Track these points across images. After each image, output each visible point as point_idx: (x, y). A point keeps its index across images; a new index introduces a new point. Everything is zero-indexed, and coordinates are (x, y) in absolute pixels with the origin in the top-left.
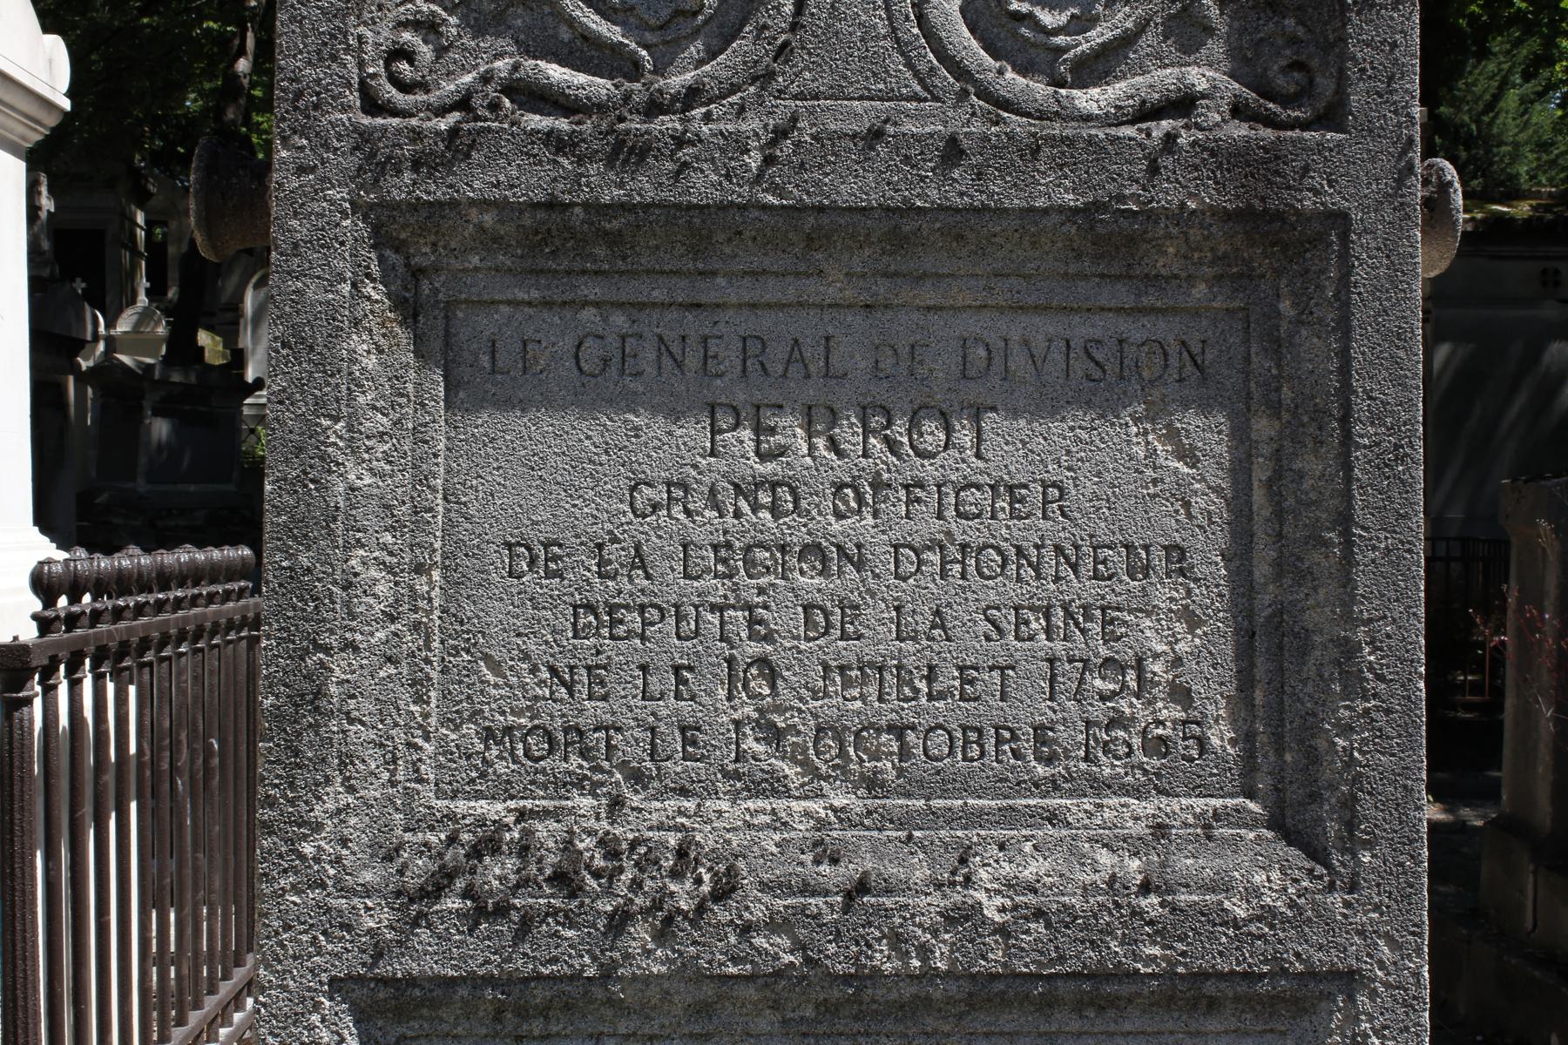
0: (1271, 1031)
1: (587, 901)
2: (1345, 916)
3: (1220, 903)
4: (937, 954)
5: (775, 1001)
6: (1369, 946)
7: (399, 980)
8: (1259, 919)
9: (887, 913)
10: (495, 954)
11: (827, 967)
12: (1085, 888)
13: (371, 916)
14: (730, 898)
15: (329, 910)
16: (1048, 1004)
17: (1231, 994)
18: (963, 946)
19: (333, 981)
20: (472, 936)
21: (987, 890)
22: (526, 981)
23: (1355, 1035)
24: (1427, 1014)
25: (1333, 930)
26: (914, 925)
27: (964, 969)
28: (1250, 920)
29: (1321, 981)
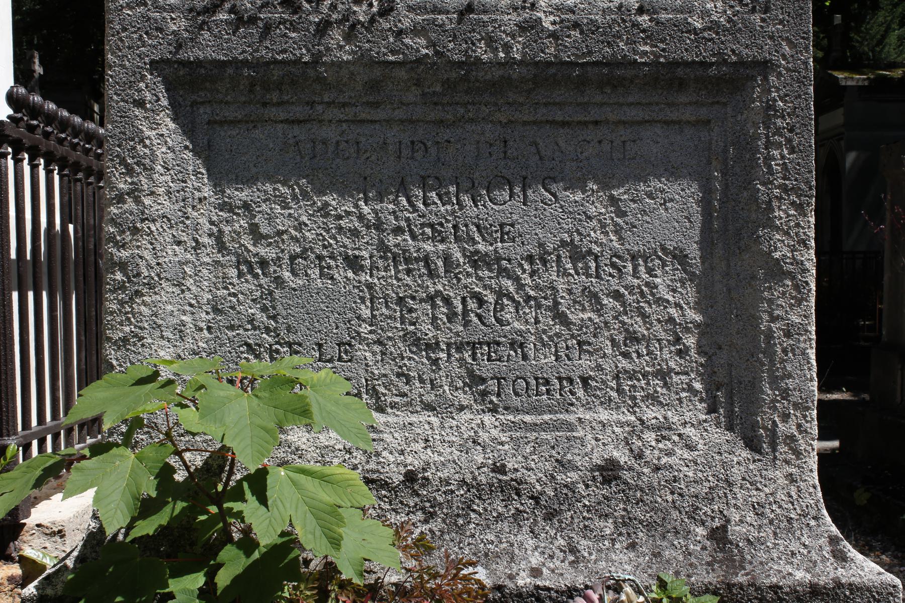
0: (718, 102)
1: (304, 15)
2: (762, 27)
3: (686, 19)
4: (515, 49)
5: (418, 80)
6: (776, 45)
7: (191, 62)
8: (710, 29)
9: (484, 24)
10: (248, 47)
11: (448, 56)
12: (604, 11)
13: (175, 23)
14: (390, 15)
15: (149, 19)
16: (581, 84)
17: (692, 77)
18: (530, 44)
19: (152, 62)
20: (234, 36)
21: (545, 12)
22: (268, 64)
23: (768, 101)
24: (812, 88)
25: (755, 35)
26: (501, 31)
27: (531, 59)
28: (704, 29)
29: (747, 68)
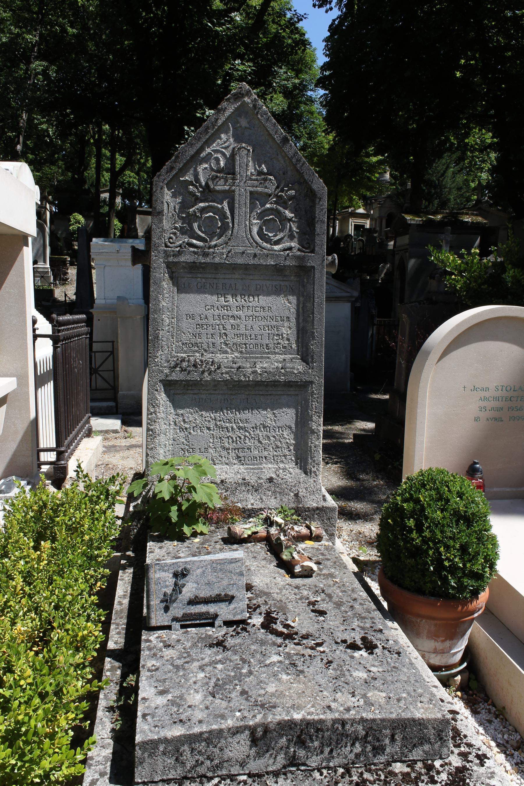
16: (267, 386)
